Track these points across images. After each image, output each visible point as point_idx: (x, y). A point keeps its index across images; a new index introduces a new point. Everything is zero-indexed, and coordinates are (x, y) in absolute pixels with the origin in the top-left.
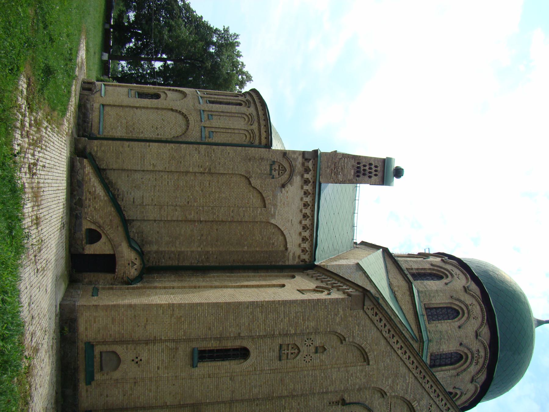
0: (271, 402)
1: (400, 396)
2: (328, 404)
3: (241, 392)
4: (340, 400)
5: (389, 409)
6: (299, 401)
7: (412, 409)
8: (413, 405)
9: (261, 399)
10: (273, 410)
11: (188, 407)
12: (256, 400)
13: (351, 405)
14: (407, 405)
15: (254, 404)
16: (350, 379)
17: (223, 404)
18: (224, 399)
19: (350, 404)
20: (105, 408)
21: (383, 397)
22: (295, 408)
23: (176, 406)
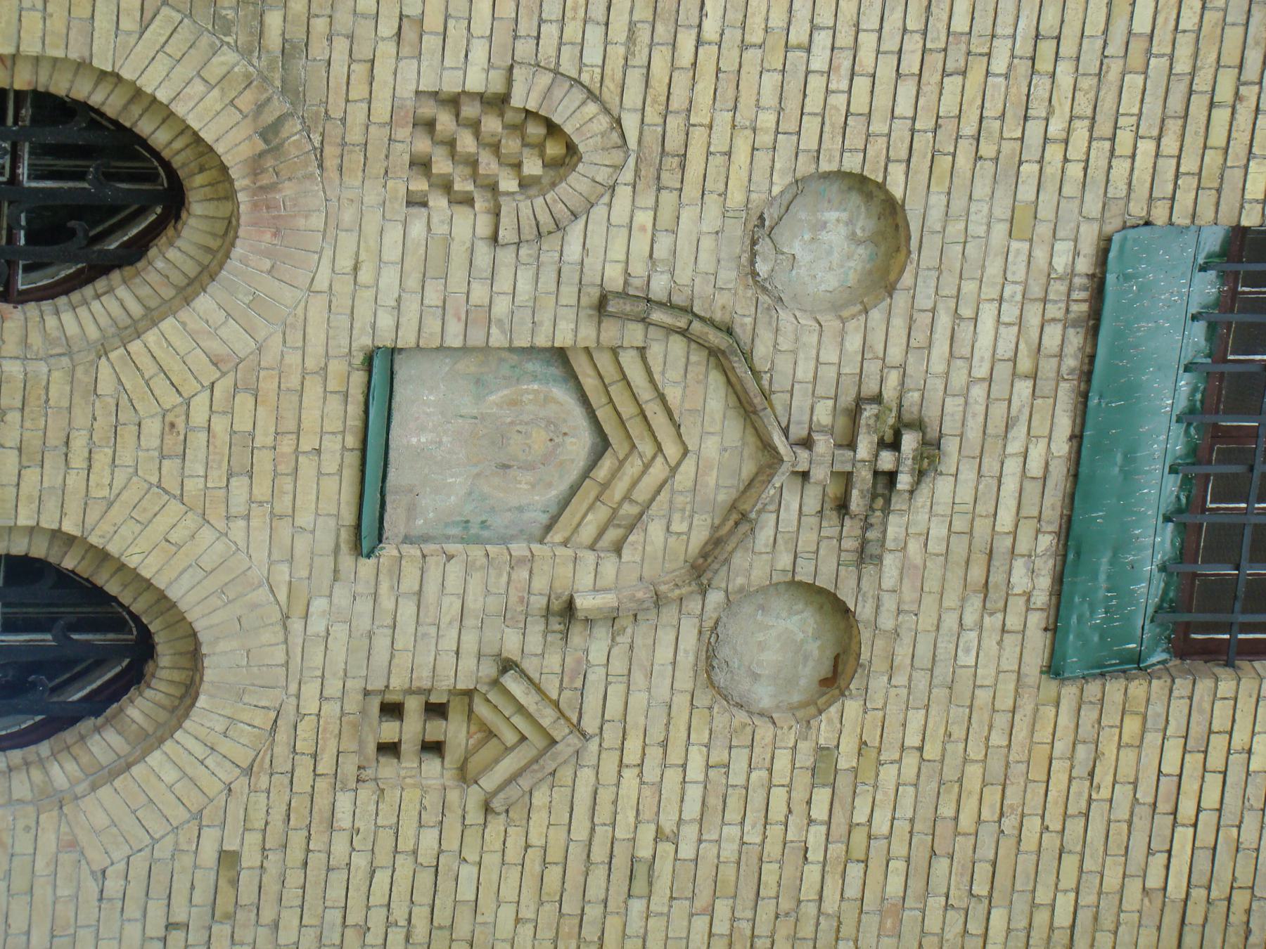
10: (1208, 58)
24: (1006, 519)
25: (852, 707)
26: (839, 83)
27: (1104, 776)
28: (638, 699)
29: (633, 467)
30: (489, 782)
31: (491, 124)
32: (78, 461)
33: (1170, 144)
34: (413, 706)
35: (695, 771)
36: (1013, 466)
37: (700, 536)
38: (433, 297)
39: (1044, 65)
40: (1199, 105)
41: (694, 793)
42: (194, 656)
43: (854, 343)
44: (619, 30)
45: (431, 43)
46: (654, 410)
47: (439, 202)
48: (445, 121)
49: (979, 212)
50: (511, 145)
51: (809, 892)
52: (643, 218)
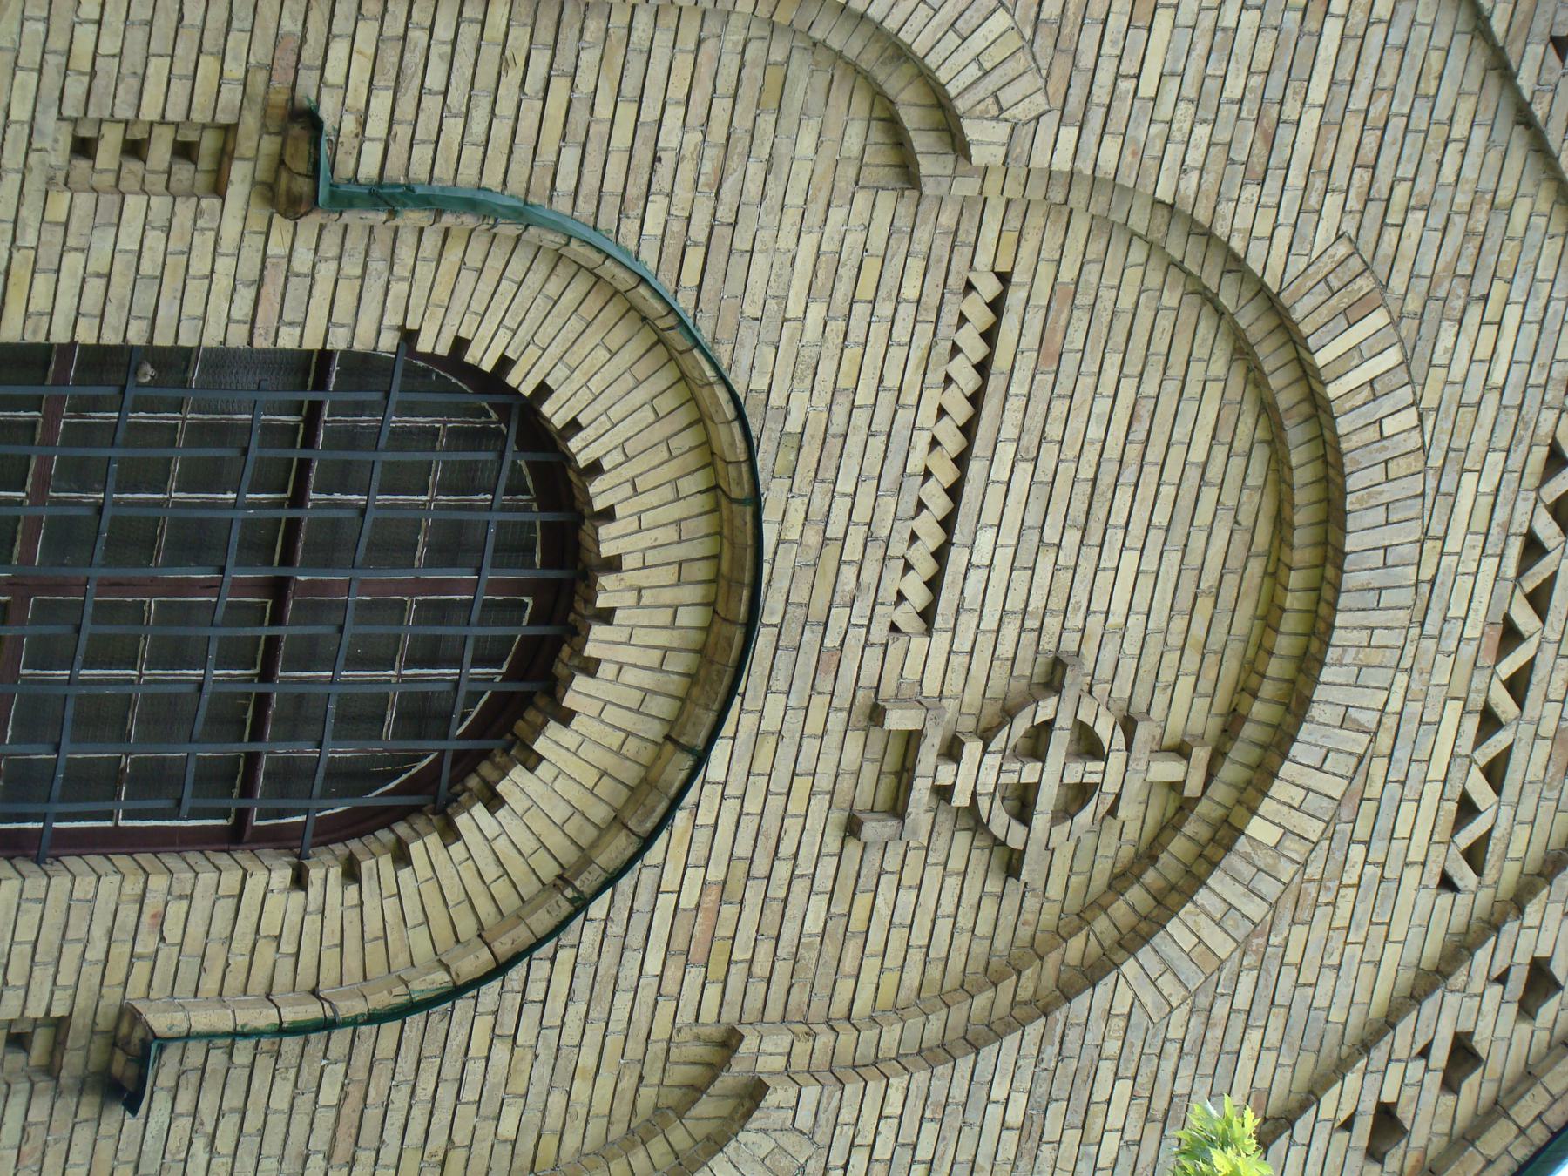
1: (1164, 193)
5: (968, 380)
7: (1296, 435)
8: (1321, 359)
14: (1242, 350)
21: (908, 174)
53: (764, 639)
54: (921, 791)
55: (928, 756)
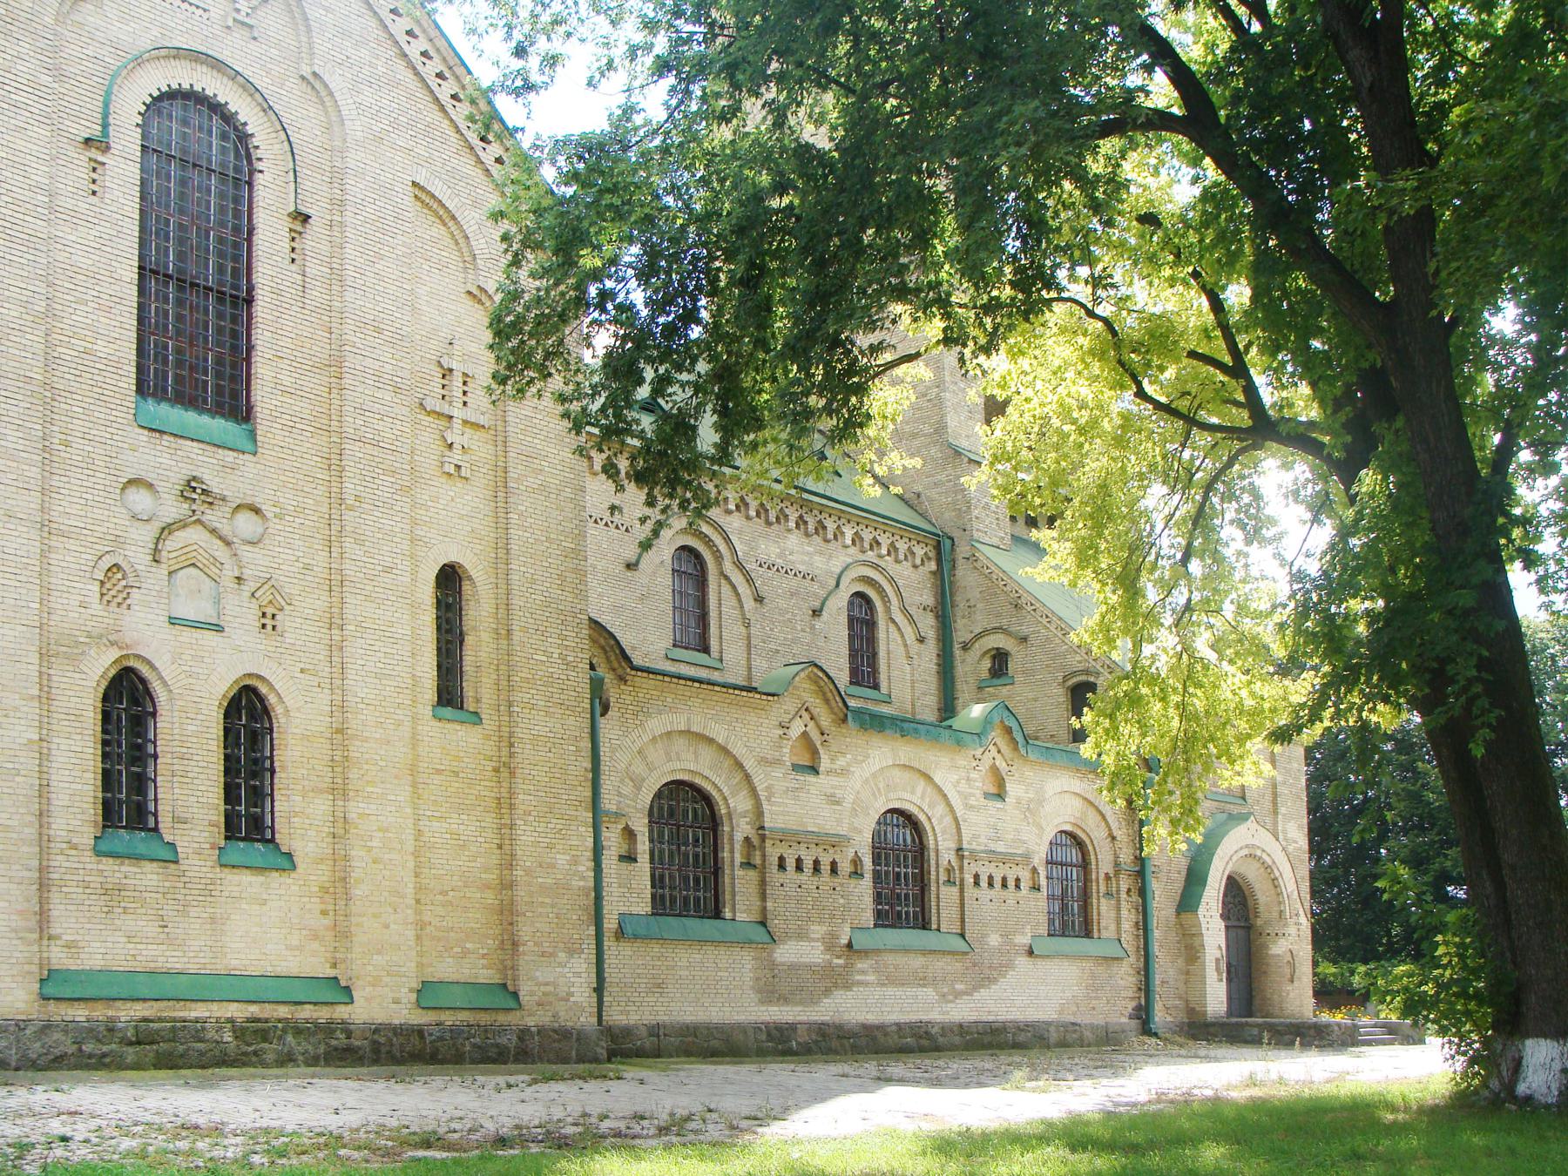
0: (63, 393)
2: (92, 199)
3: (14, 489)
4: (88, 154)
6: (72, 299)
9: (48, 425)
10: (91, 394)
11: (52, 672)
12: (47, 444)
13: (111, 121)
15: (62, 454)
16: (13, 96)
17: (52, 556)
18: (33, 549)
19: (105, 126)
20: (36, 936)
22: (95, 318)
23: (46, 713)
24: (215, 461)
25: (263, 507)
26: (96, 492)
27: (283, 444)
28: (261, 562)
29: (199, 557)
30: (283, 603)
31: (108, 586)
32: (199, 700)
33: (113, 406)
34: (263, 621)
35: (281, 550)
36: (200, 458)
37: (219, 542)
38: (155, 605)
39: (91, 437)
40: (102, 398)
41: (287, 551)
42: (250, 675)
43: (166, 496)
44: (83, 550)
45: (86, 599)
46: (185, 550)
47: (128, 601)
48: (106, 598)
49: (131, 459)
50: (114, 581)
51: (312, 524)
52: (133, 548)
53: (210, 53)
54: (247, 20)
55: (239, 18)
